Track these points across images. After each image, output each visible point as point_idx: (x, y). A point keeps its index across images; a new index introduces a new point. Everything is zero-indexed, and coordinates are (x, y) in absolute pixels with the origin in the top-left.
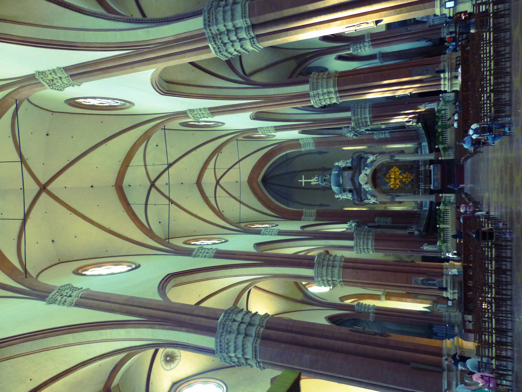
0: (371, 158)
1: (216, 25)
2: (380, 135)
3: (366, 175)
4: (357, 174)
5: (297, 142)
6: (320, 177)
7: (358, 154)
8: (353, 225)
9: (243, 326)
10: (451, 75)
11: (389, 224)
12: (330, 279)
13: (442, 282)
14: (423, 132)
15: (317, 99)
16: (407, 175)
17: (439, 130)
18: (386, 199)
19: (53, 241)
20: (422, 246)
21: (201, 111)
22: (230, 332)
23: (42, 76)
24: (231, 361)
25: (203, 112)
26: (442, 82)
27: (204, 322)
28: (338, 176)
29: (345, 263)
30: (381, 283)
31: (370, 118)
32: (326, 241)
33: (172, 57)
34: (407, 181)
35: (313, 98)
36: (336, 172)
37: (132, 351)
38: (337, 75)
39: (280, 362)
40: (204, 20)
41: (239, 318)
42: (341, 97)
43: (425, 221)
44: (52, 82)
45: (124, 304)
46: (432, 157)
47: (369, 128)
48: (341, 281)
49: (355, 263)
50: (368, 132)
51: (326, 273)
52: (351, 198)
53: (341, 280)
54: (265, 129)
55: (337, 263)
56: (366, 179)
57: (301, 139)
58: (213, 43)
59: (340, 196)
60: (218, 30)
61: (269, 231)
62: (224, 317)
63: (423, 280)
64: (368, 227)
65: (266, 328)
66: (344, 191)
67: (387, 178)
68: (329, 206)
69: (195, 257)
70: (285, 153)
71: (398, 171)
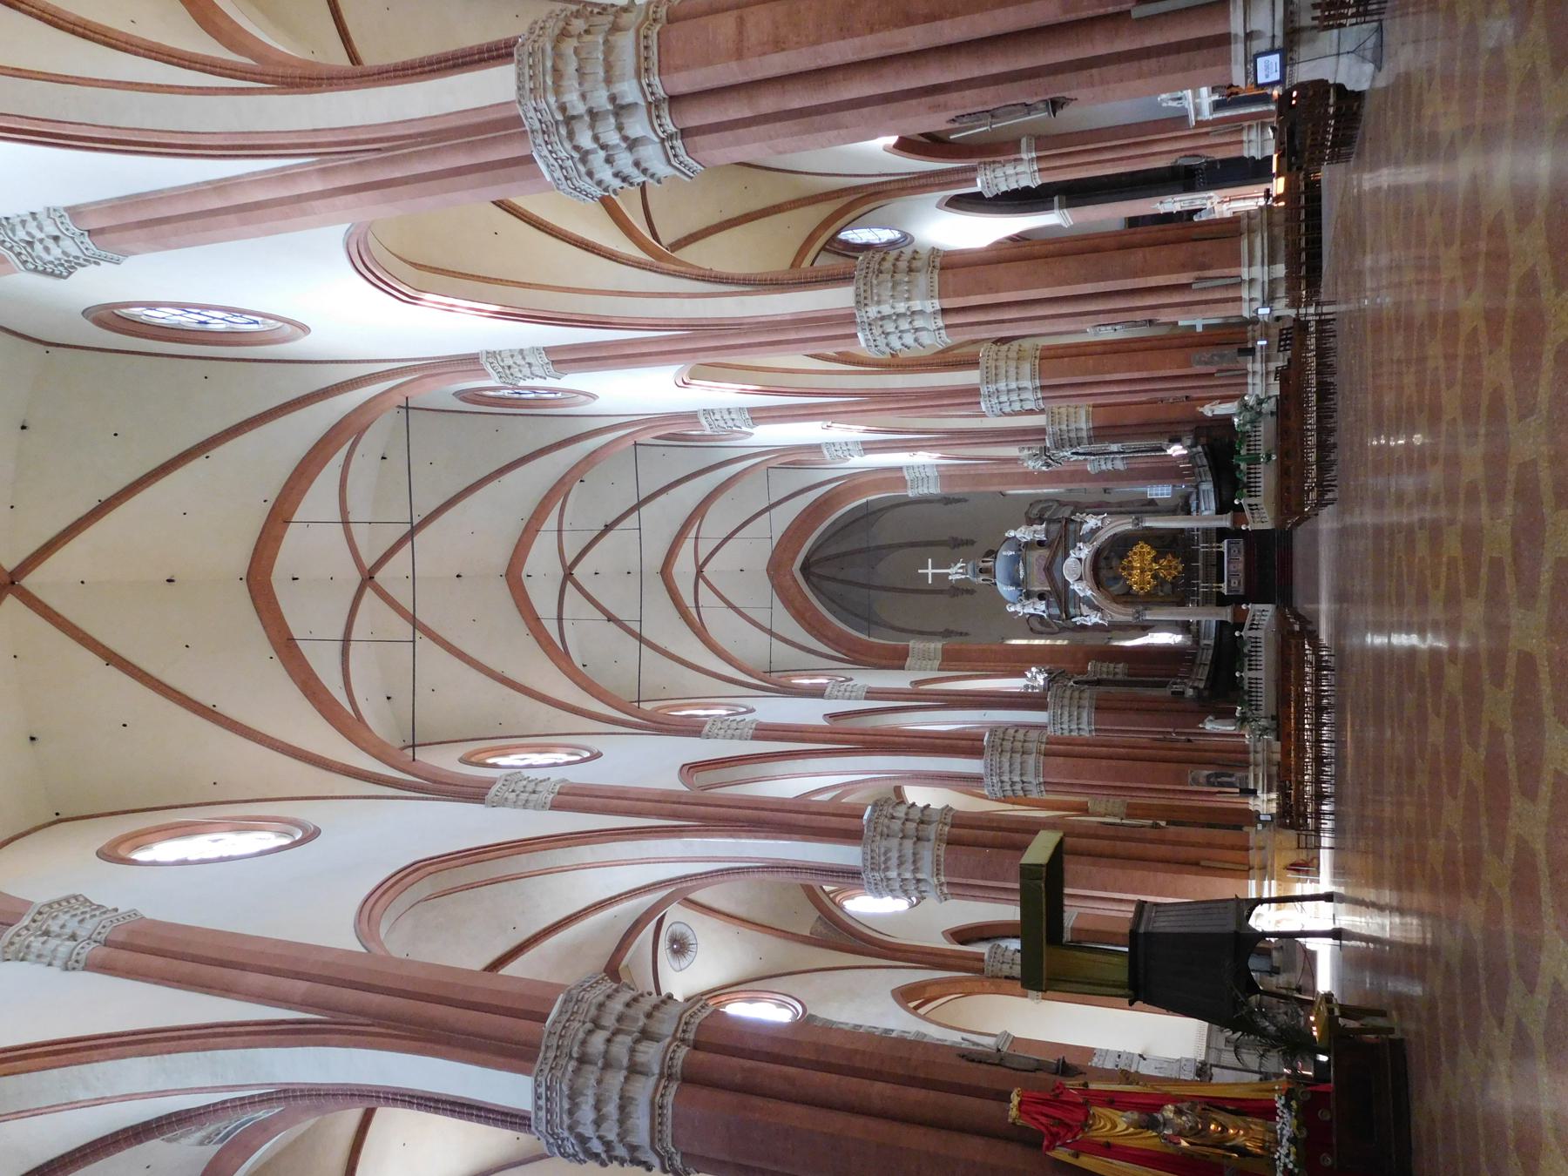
0: (1092, 522)
1: (879, 303)
2: (1102, 462)
3: (1080, 559)
4: (1059, 559)
5: (899, 475)
6: (971, 563)
7: (1041, 506)
8: (1041, 680)
9: (911, 826)
10: (1266, 368)
11: (1119, 677)
12: (1017, 779)
13: (1247, 778)
14: (1205, 461)
15: (995, 401)
16: (1169, 561)
17: (1243, 466)
18: (1123, 614)
19: (389, 698)
20: (1202, 722)
21: (730, 413)
22: (888, 836)
23: (491, 360)
24: (887, 886)
25: (733, 416)
26: (1250, 380)
27: (835, 822)
28: (1014, 560)
29: (1048, 746)
30: (1125, 784)
31: (1088, 430)
32: (983, 712)
33: (781, 347)
34: (1170, 574)
35: (987, 399)
36: (1011, 553)
37: (689, 884)
38: (1038, 353)
39: (982, 878)
40: (857, 295)
41: (901, 812)
42: (1043, 398)
43: (1207, 668)
44: (507, 371)
45: (659, 801)
46: (1225, 522)
47: (1081, 451)
48: (1040, 784)
49: (1068, 744)
50: (1075, 457)
51: (1011, 765)
52: (1044, 612)
53: (1041, 780)
54: (838, 448)
55: (1032, 746)
56: (1079, 569)
57: (908, 467)
58: (868, 333)
59: (1018, 608)
60: (879, 312)
61: (842, 688)
62: (873, 811)
63: (1208, 777)
64: (1075, 682)
65: (952, 826)
66: (1028, 595)
67: (1124, 569)
68: (966, 634)
69: (708, 737)
70: (864, 500)
71: (1149, 553)
